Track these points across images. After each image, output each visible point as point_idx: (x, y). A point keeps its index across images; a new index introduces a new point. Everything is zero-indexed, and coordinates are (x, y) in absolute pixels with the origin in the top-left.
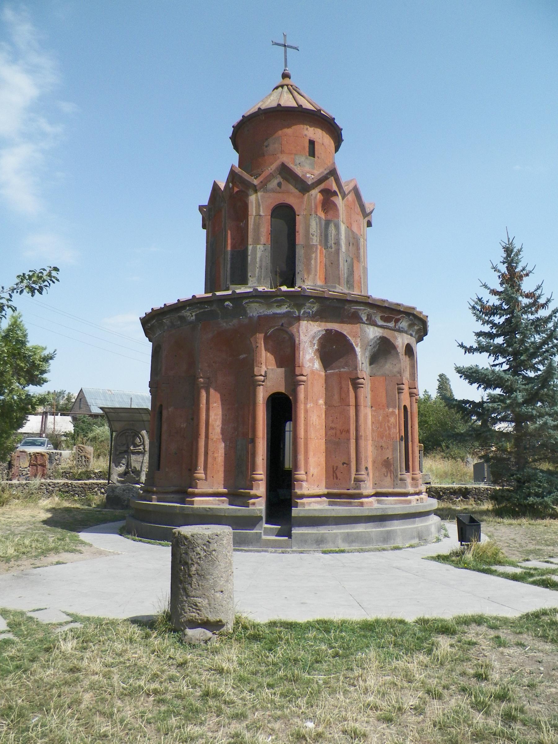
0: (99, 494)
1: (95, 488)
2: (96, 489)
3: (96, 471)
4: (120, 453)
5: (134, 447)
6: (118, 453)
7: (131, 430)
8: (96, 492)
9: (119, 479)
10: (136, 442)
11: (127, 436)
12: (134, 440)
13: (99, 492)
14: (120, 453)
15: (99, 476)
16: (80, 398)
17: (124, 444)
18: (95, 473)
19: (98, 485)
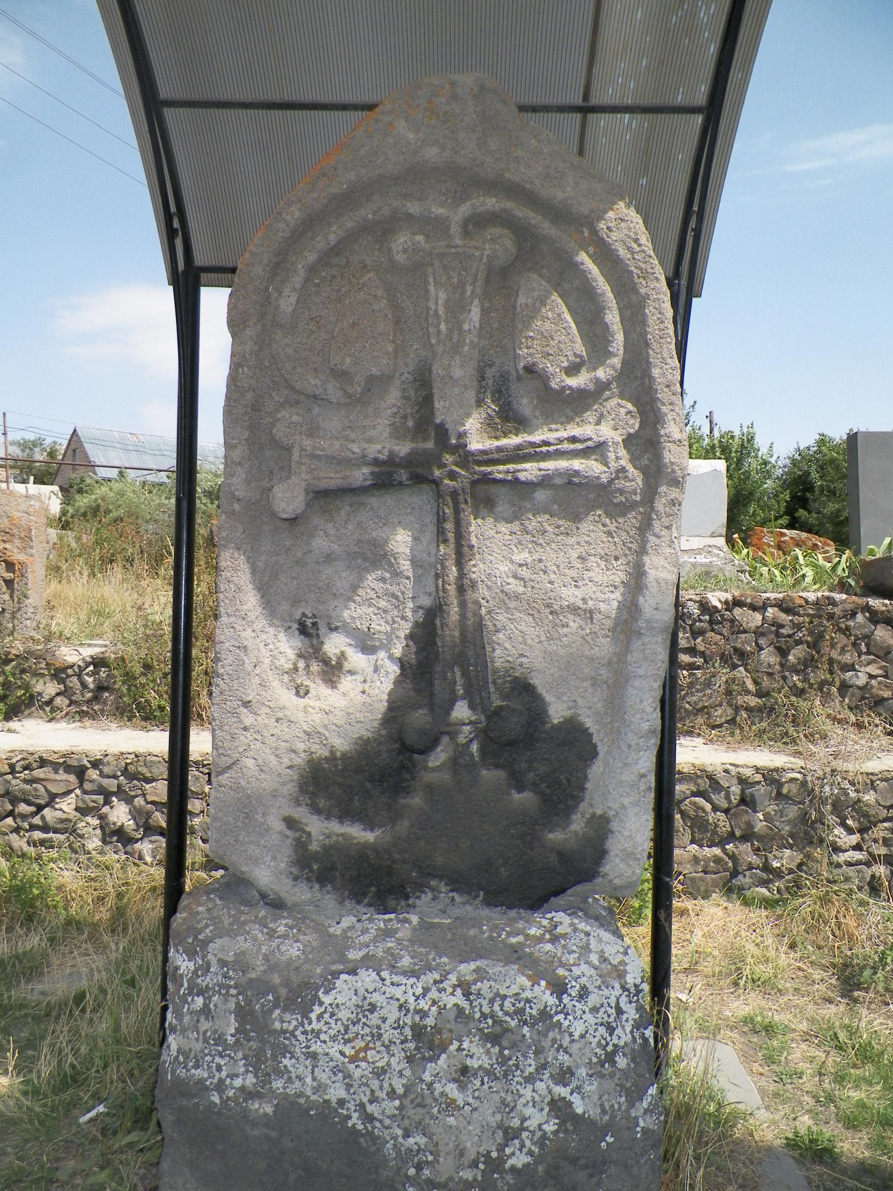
0: (94, 843)
1: (53, 797)
2: (67, 806)
3: (69, 655)
4: (324, 498)
5: (509, 418)
6: (288, 498)
7: (464, 181)
8: (67, 827)
9: (321, 829)
10: (528, 352)
11: (417, 270)
12: (506, 323)
13: (89, 824)
14: (324, 498)
15: (102, 691)
16: (72, 447)
17: (376, 384)
18: (59, 673)
19: (80, 773)
